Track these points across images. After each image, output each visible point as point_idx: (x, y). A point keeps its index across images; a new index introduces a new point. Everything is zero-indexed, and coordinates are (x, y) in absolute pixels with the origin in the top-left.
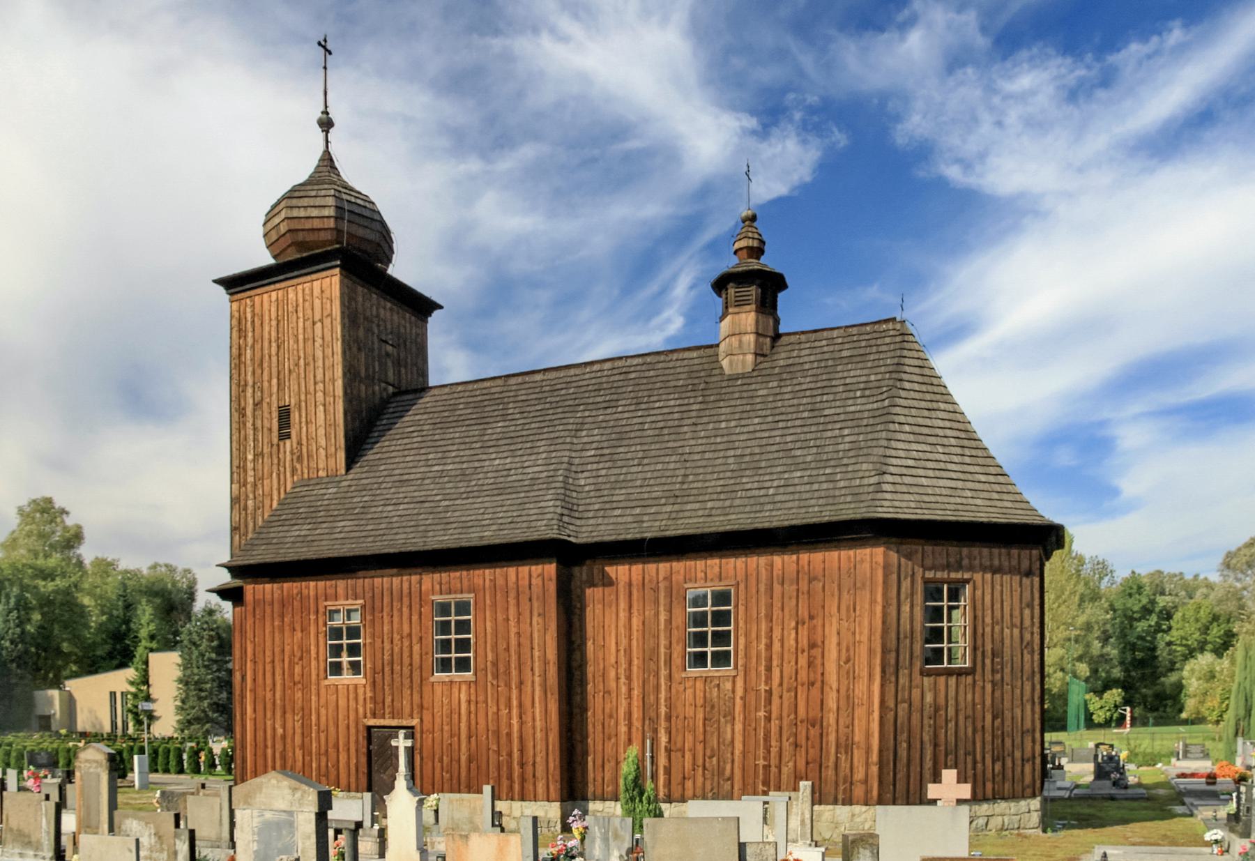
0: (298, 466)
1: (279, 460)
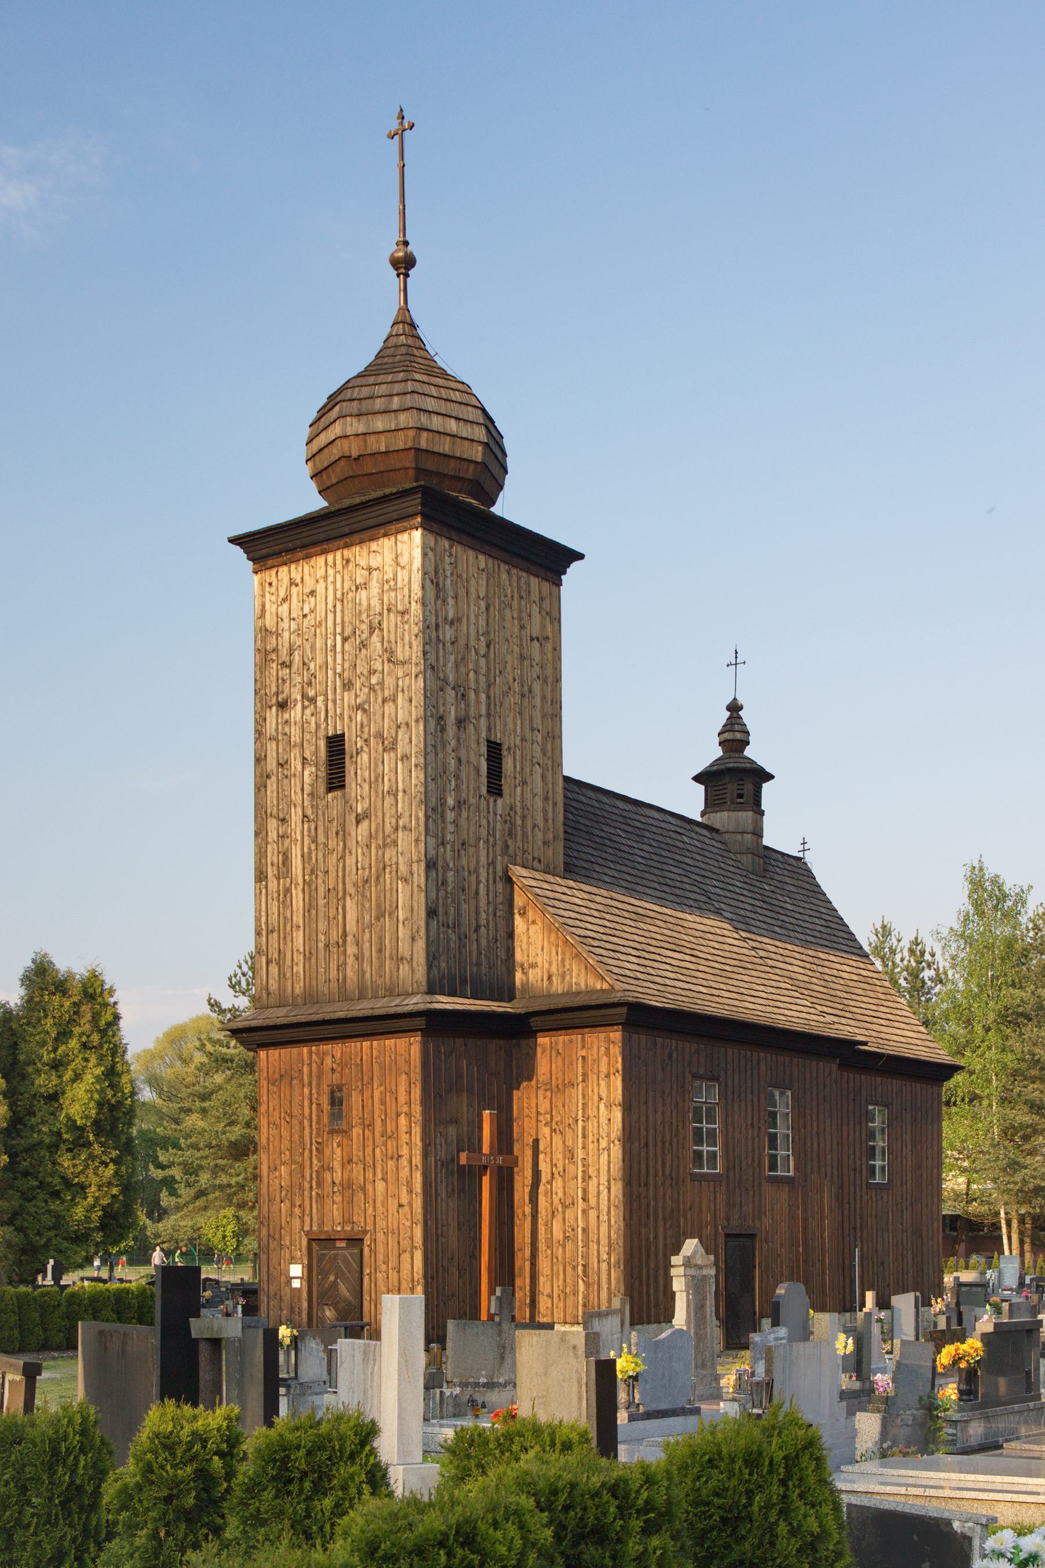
0: (510, 842)
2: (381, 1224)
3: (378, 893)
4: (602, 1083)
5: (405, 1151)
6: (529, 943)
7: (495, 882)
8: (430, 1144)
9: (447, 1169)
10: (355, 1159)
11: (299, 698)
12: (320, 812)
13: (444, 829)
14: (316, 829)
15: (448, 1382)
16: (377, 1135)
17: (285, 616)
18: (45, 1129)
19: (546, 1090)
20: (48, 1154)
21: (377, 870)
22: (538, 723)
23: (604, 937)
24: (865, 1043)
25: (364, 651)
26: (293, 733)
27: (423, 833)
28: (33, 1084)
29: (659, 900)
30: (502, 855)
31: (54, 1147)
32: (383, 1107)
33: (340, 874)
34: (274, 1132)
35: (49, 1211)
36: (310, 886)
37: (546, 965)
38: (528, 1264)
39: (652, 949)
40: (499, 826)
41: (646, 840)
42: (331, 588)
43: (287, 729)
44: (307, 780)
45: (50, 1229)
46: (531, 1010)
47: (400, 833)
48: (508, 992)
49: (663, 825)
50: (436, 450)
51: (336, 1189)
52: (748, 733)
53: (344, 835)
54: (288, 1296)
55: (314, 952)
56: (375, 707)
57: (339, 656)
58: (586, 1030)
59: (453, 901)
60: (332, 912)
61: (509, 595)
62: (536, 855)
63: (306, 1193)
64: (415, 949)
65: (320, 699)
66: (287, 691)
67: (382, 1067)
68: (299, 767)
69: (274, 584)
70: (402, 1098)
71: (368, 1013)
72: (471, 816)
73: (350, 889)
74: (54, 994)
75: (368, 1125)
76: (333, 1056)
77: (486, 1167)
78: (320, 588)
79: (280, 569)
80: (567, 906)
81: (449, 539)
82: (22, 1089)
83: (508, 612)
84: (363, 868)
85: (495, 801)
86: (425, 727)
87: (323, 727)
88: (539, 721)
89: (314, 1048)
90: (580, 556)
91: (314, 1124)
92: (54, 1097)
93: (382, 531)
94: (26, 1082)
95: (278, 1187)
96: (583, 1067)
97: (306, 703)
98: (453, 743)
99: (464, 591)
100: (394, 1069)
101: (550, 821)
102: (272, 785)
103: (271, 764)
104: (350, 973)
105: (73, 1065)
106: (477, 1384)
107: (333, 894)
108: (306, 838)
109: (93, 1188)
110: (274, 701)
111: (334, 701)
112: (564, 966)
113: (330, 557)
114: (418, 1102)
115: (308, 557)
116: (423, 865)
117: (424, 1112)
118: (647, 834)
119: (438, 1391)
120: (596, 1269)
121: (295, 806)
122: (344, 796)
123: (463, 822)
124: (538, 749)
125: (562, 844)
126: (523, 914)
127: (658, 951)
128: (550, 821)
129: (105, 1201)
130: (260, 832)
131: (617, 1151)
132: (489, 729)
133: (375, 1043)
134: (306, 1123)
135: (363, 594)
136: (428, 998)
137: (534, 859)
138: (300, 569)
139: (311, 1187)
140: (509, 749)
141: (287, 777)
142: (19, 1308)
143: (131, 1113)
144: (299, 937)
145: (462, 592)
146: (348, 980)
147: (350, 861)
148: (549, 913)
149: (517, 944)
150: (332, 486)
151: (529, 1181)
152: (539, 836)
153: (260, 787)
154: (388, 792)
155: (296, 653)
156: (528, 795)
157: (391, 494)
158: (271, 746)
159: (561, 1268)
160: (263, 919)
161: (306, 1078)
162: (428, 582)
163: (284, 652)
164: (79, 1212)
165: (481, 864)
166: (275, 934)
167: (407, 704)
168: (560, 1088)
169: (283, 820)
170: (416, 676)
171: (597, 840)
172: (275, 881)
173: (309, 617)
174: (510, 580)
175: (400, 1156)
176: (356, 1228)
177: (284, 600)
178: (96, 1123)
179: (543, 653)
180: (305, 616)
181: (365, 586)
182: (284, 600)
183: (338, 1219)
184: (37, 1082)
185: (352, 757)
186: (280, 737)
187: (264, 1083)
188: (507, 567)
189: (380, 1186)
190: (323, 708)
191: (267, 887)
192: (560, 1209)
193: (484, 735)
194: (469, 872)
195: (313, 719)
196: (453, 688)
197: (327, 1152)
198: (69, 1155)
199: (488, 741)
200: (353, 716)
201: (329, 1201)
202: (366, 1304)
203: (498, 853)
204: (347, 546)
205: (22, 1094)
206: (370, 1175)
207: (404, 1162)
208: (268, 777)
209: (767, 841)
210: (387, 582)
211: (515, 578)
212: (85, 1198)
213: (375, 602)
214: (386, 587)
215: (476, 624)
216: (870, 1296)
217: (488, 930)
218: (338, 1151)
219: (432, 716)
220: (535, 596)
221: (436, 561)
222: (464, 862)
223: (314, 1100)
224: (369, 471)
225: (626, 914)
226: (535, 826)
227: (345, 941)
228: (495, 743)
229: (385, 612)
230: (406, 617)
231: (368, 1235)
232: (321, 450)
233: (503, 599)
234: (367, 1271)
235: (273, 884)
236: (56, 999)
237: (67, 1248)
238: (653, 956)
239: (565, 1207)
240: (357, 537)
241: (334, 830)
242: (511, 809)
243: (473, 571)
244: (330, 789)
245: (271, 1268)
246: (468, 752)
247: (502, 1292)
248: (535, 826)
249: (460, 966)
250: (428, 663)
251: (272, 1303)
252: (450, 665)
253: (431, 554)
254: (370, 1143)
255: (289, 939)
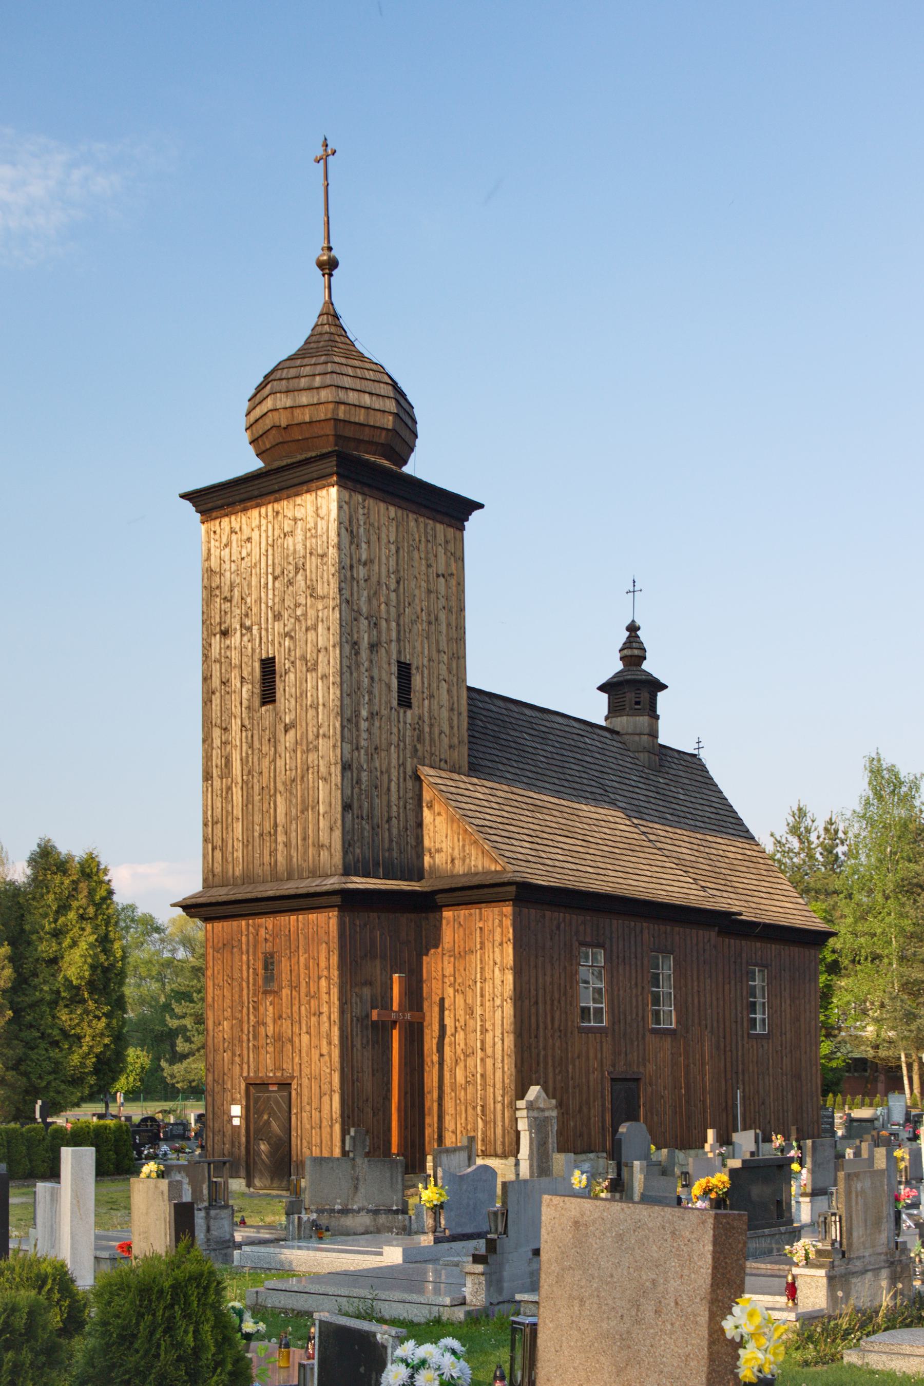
0: (419, 746)
1: (399, 730)
2: (306, 1071)
3: (302, 790)
4: (497, 950)
5: (325, 1009)
6: (435, 832)
7: (405, 780)
8: (346, 1003)
9: (362, 1025)
10: (284, 1016)
11: (238, 627)
12: (255, 722)
13: (358, 736)
14: (252, 736)
15: (306, 1209)
16: (303, 994)
17: (227, 559)
18: (46, 988)
19: (450, 956)
20: (48, 1010)
21: (302, 771)
22: (443, 645)
23: (501, 826)
24: (741, 914)
25: (291, 588)
26: (233, 657)
27: (339, 740)
28: (36, 950)
29: (557, 794)
30: (411, 758)
31: (54, 1004)
32: (307, 972)
33: (272, 775)
34: (217, 992)
35: (49, 1058)
36: (247, 785)
37: (450, 850)
38: (435, 1105)
39: (546, 836)
40: (408, 733)
41: (550, 742)
42: (264, 535)
43: (228, 654)
44: (245, 695)
45: (50, 1073)
46: (435, 888)
47: (321, 740)
48: (417, 873)
49: (567, 729)
50: (352, 420)
51: (268, 1041)
52: (644, 650)
53: (275, 742)
54: (230, 1132)
55: (250, 840)
56: (299, 635)
57: (270, 593)
58: (483, 905)
59: (367, 797)
60: (266, 806)
61: (417, 540)
62: (443, 757)
63: (245, 1045)
64: (333, 837)
65: (255, 628)
66: (228, 621)
67: (306, 937)
68: (239, 685)
69: (218, 532)
70: (323, 964)
71: (292, 892)
72: (383, 725)
73: (280, 787)
74: (56, 873)
75: (294, 987)
76: (266, 928)
77: (395, 1022)
78: (255, 535)
79: (223, 520)
80: (468, 800)
81: (363, 494)
82: (28, 954)
83: (416, 555)
84: (291, 770)
85: (405, 712)
86: (341, 651)
87: (257, 651)
88: (445, 645)
89: (251, 921)
90: (481, 506)
91: (251, 985)
92: (54, 961)
93: (305, 488)
94: (31, 948)
95: (222, 1039)
96: (481, 937)
97: (244, 631)
98: (366, 664)
99: (376, 537)
100: (316, 939)
101: (456, 728)
102: (216, 699)
103: (216, 682)
104: (280, 858)
105: (71, 934)
106: (333, 1211)
107: (266, 791)
108: (244, 744)
109: (88, 1039)
110: (218, 629)
111: (267, 630)
112: (464, 851)
113: (263, 510)
114: (336, 967)
115: (245, 510)
116: (339, 767)
117: (341, 976)
118: (551, 737)
119: (296, 1216)
120: (492, 1109)
121: (235, 717)
122: (275, 709)
123: (375, 730)
124: (445, 667)
125: (466, 747)
126: (430, 807)
127: (551, 837)
128: (456, 728)
129: (98, 1050)
130: (207, 739)
131: (509, 1009)
132: (399, 652)
133: (300, 917)
134: (244, 984)
135: (290, 540)
136: (343, 879)
137: (441, 760)
138: (239, 519)
139: (249, 1040)
140: (417, 668)
141: (228, 693)
142: (9, 1142)
143: (122, 976)
144: (238, 827)
145: (374, 538)
146: (279, 864)
147: (280, 763)
148: (451, 806)
149: (425, 832)
150: (267, 450)
151: (436, 1034)
152: (446, 741)
153: (207, 701)
154: (311, 706)
155: (236, 590)
156: (435, 707)
157: (311, 458)
158: (216, 667)
159: (463, 1108)
160: (209, 813)
161: (244, 947)
162: (343, 530)
163: (226, 589)
164: (75, 1059)
165: (392, 765)
166: (219, 825)
167: (326, 632)
168: (461, 955)
169: (226, 729)
170: (333, 609)
171: (503, 742)
172: (219, 780)
173: (246, 559)
174: (418, 527)
175: (321, 1013)
176: (285, 1074)
177: (226, 545)
178: (91, 983)
179: (448, 587)
180: (243, 559)
181: (292, 533)
182: (226, 545)
183: (271, 1067)
184: (39, 948)
185: (281, 676)
186: (223, 660)
187: (211, 951)
188: (415, 516)
189: (305, 1038)
190: (258, 636)
191: (212, 786)
192: (462, 1058)
193: (394, 657)
194: (382, 772)
195: (250, 644)
196: (366, 618)
197: (262, 1009)
198: (66, 1010)
199: (399, 662)
200: (282, 642)
201: (263, 1052)
202: (293, 1139)
203: (408, 755)
204: (277, 500)
205: (27, 958)
206: (296, 1030)
207: (324, 1018)
208: (213, 693)
209: (662, 740)
210: (309, 530)
211: (422, 525)
212: (81, 1047)
213: (299, 547)
214: (309, 534)
215: (387, 565)
216: (711, 1134)
217: (399, 821)
218: (271, 1009)
219: (347, 642)
220: (441, 539)
221: (350, 512)
222: (377, 765)
223: (251, 966)
224: (297, 438)
225: (524, 806)
226: (441, 732)
227: (276, 831)
228: (405, 663)
229: (308, 555)
230: (325, 559)
231: (295, 1081)
232: (257, 421)
233: (411, 542)
234: (294, 1111)
235: (217, 783)
236: (58, 878)
237: (64, 1090)
238: (545, 842)
239: (466, 1056)
240: (285, 493)
241: (267, 737)
242: (420, 718)
243: (384, 520)
244: (263, 703)
245: (216, 1109)
246: (379, 671)
247: (356, 1132)
248: (441, 732)
249: (373, 851)
250: (344, 597)
251: (216, 1138)
252: (363, 599)
253: (345, 507)
254: (297, 1002)
255: (230, 829)
